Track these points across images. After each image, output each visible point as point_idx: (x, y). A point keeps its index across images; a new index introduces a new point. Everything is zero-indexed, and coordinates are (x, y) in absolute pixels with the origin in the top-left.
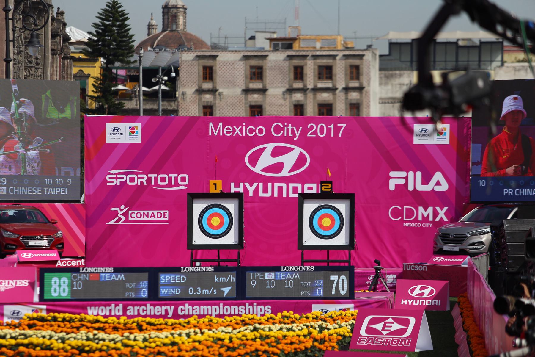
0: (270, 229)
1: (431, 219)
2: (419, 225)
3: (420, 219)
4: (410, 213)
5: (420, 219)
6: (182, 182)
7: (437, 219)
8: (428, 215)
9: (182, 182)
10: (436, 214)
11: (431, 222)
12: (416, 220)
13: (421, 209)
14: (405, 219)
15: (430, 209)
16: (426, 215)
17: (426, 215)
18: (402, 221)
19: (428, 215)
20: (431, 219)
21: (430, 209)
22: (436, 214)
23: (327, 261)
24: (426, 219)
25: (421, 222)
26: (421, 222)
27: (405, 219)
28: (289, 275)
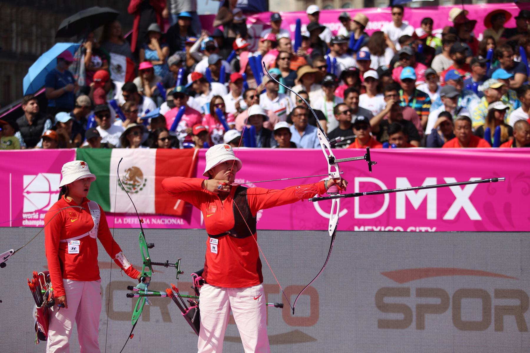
1: (432, 214)
3: (401, 213)
4: (372, 197)
5: (401, 213)
7: (451, 215)
8: (424, 202)
10: (446, 199)
11: (431, 223)
12: (389, 217)
14: (357, 215)
16: (416, 204)
17: (416, 204)
19: (424, 202)
20: (432, 214)
22: (446, 199)
24: (416, 215)
26: (404, 223)
27: (357, 215)
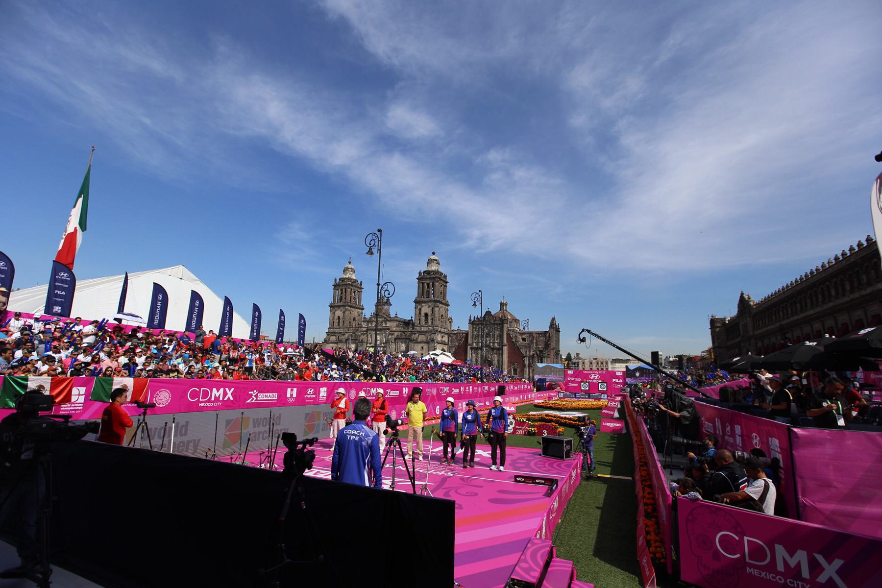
0: (594, 387)
1: (221, 399)
2: (211, 404)
3: (213, 399)
4: (206, 394)
5: (213, 399)
6: (580, 380)
9: (580, 380)
12: (209, 401)
13: (214, 390)
15: (222, 390)
18: (199, 402)
20: (221, 399)
21: (222, 390)
22: (225, 394)
23: (603, 392)
24: (217, 399)
25: (213, 402)
28: (597, 394)
